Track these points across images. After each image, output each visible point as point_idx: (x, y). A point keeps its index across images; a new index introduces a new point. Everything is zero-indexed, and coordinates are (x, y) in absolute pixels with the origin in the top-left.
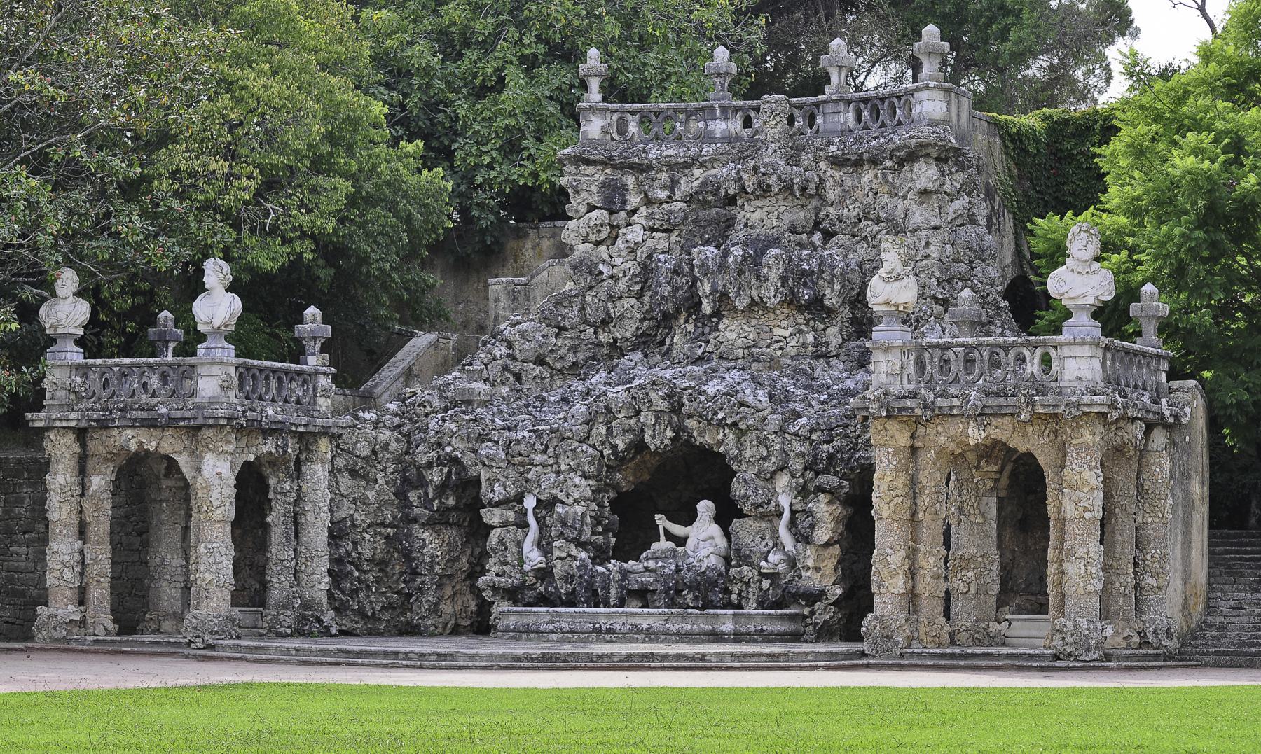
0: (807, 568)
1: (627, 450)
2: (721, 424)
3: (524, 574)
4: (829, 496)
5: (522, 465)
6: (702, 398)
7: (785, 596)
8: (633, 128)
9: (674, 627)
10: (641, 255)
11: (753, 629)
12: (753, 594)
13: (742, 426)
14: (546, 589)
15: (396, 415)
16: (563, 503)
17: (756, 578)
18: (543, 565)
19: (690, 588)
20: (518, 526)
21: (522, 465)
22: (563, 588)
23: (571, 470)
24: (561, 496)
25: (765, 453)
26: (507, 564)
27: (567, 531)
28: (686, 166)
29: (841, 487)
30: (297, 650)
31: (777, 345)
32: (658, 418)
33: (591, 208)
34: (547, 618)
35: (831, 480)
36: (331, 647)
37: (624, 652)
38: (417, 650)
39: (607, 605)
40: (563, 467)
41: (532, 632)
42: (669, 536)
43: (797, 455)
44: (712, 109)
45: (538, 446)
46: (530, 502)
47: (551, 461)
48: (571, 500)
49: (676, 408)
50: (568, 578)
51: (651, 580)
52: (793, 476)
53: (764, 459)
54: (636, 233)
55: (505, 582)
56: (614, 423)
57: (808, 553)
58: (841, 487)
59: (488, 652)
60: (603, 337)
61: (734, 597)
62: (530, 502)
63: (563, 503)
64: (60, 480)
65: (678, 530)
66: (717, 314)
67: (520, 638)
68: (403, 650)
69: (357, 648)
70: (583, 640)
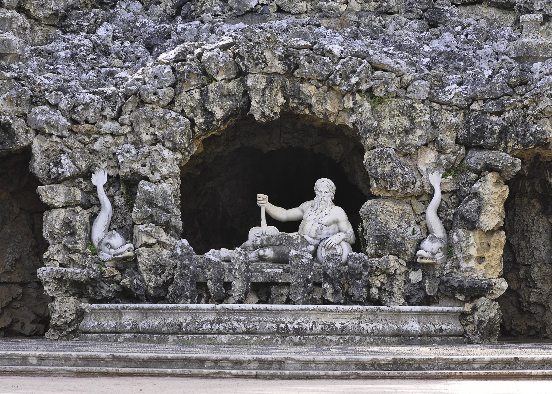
0: (468, 258)
1: (225, 119)
2: (354, 90)
3: (102, 263)
4: (497, 175)
5: (88, 134)
6: (327, 60)
7: (438, 288)
9: (369, 328)
11: (432, 329)
12: (398, 286)
13: (378, 93)
14: (131, 282)
16: (147, 179)
17: (403, 269)
18: (131, 254)
19: (331, 281)
20: (85, 207)
21: (88, 134)
22: (152, 281)
23: (156, 141)
25: (407, 124)
26: (75, 251)
27: (157, 213)
29: (513, 165)
30: (41, 359)
32: (270, 82)
34: (211, 317)
35: (502, 157)
36: (103, 355)
37: (487, 357)
38: (233, 357)
40: (145, 137)
41: (187, 333)
42: (271, 221)
43: (450, 127)
45: (108, 112)
46: (99, 179)
48: (157, 176)
50: (158, 268)
51: (280, 271)
52: (441, 151)
53: (407, 131)
55: (74, 272)
57: (472, 240)
58: (513, 165)
59: (328, 358)
61: (375, 291)
62: (99, 179)
63: (147, 179)
65: (280, 213)
67: (165, 341)
68: (214, 356)
69: (145, 355)
70: (264, 343)
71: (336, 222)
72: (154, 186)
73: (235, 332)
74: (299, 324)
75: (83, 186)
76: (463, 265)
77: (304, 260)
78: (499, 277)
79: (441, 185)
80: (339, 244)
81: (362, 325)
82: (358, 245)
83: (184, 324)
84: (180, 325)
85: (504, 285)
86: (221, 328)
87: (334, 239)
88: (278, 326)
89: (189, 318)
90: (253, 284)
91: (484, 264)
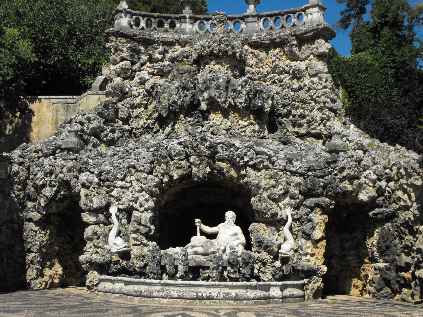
5: (108, 187)
8: (143, 24)
10: (148, 85)
15: (20, 157)
16: (138, 210)
21: (108, 187)
22: (138, 264)
24: (137, 206)
28: (171, 44)
31: (243, 130)
33: (123, 59)
39: (172, 277)
41: (144, 296)
42: (203, 233)
44: (185, 18)
46: (113, 210)
47: (129, 185)
48: (142, 209)
49: (212, 157)
53: (274, 187)
54: (145, 74)
60: (126, 127)
63: (138, 210)
66: (208, 111)
71: (236, 234)
72: (140, 214)
74: (210, 293)
75: (105, 213)
77: (217, 254)
78: (323, 264)
79: (292, 215)
80: (237, 246)
81: (248, 294)
82: (248, 246)
83: (143, 291)
84: (141, 292)
85: (325, 269)
86: (163, 294)
87: (234, 243)
88: (197, 294)
90: (190, 267)
91: (315, 257)
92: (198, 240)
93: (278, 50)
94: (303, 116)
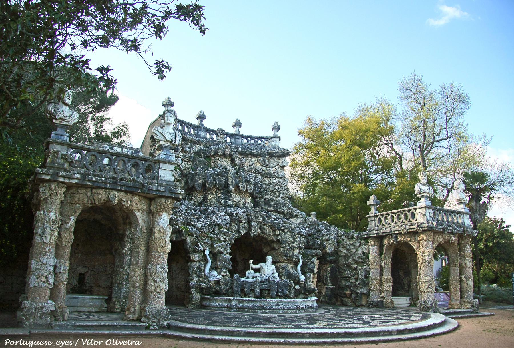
16: (223, 253)
24: (222, 250)
26: (201, 277)
34: (275, 304)
40: (222, 239)
41: (266, 309)
42: (252, 269)
53: (293, 243)
56: (241, 224)
62: (207, 252)
64: (52, 216)
73: (284, 309)
76: (309, 284)
89: (266, 304)
92: (250, 273)
93: (254, 159)
94: (271, 200)
